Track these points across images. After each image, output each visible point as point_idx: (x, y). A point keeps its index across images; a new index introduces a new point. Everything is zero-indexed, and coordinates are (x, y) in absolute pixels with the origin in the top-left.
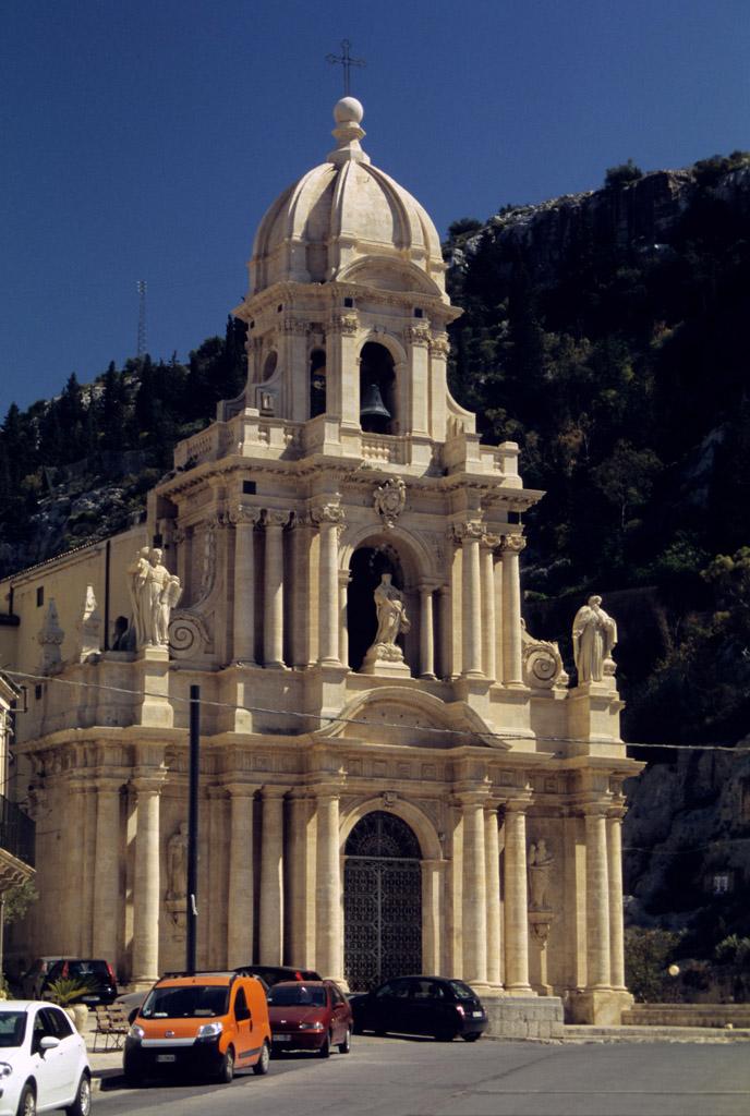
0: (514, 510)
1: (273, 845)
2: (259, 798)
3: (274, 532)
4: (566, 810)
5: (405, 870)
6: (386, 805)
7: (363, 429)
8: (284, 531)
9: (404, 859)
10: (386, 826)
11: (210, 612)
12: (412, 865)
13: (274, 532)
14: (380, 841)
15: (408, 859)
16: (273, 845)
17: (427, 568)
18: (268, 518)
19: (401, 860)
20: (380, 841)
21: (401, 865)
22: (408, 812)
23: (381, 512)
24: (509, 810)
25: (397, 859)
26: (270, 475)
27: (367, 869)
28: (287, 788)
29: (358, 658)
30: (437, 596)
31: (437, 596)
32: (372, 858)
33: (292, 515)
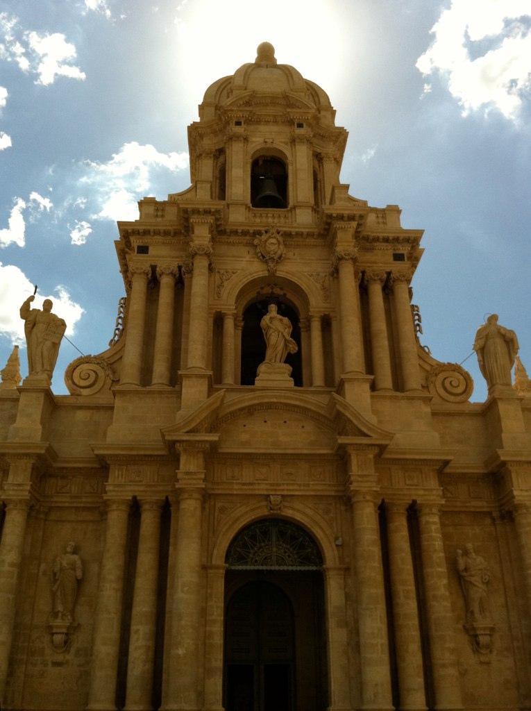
0: (397, 252)
1: (146, 560)
2: (135, 509)
3: (166, 283)
4: (495, 514)
6: (271, 509)
7: (253, 206)
8: (176, 284)
11: (118, 357)
13: (166, 283)
14: (275, 549)
16: (146, 560)
17: (316, 304)
20: (275, 549)
22: (299, 513)
23: (264, 257)
26: (159, 238)
29: (248, 376)
30: (326, 323)
31: (326, 323)
33: (180, 268)
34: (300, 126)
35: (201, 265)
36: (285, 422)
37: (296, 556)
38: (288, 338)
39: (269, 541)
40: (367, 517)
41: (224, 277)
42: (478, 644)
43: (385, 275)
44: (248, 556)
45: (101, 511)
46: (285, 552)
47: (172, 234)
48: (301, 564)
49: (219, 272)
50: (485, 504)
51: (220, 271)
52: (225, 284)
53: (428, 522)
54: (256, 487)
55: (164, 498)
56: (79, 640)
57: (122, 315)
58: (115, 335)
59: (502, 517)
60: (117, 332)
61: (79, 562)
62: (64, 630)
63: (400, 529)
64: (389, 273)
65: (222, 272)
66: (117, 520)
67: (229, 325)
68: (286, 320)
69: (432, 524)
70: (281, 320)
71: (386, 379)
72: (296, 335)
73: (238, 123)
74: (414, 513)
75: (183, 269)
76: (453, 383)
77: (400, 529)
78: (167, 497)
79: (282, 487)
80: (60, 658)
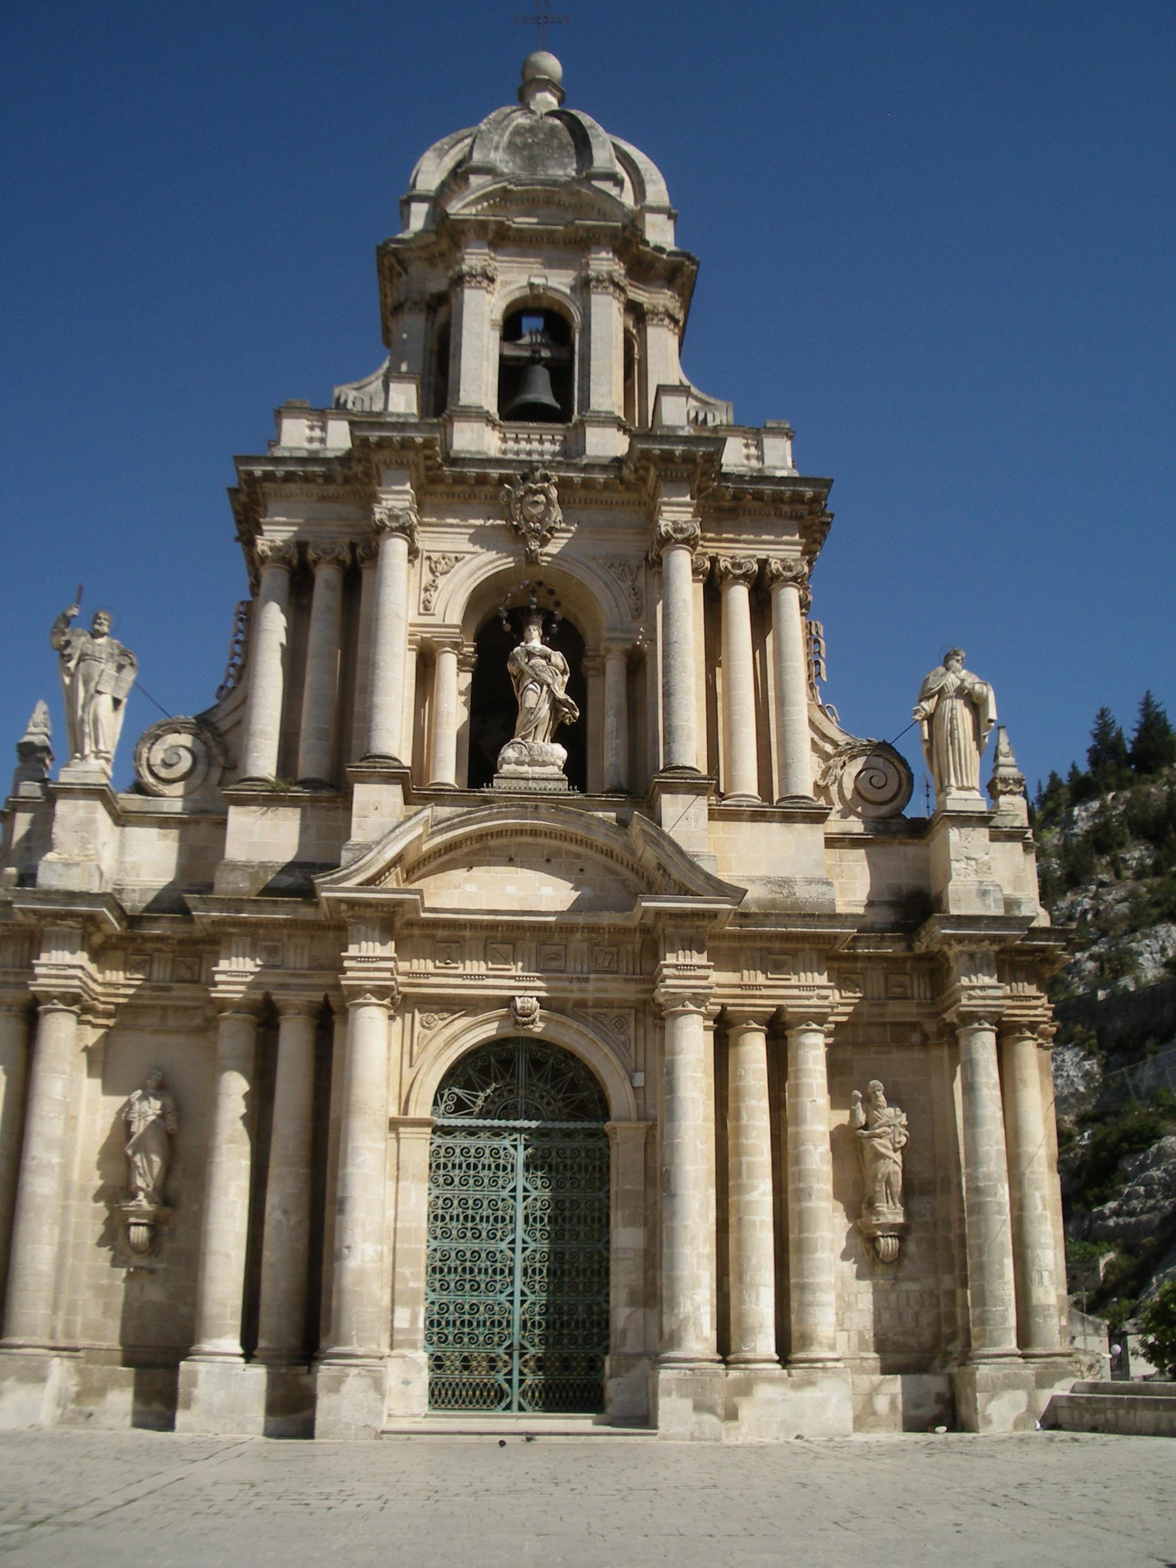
3: (325, 577)
4: (931, 1027)
5: (575, 1145)
9: (572, 1125)
10: (536, 1064)
12: (591, 1134)
15: (579, 1125)
18: (311, 555)
19: (564, 1125)
21: (568, 1134)
24: (790, 1026)
25: (557, 1125)
27: (496, 1143)
28: (319, 997)
32: (503, 1123)
33: (353, 547)
35: (396, 548)
36: (548, 860)
37: (560, 1104)
38: (561, 694)
39: (512, 1075)
41: (440, 568)
42: (877, 1252)
43: (756, 567)
44: (474, 1103)
46: (542, 1097)
48: (572, 1117)
49: (429, 558)
50: (914, 1010)
51: (432, 555)
52: (441, 581)
55: (321, 999)
57: (241, 637)
58: (229, 676)
59: (940, 1033)
60: (232, 670)
64: (763, 563)
65: (434, 556)
67: (448, 663)
68: (558, 658)
70: (547, 658)
72: (577, 687)
75: (359, 551)
76: (873, 780)
78: (326, 997)
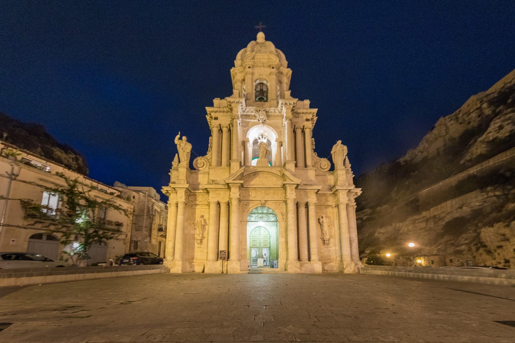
3: (225, 130)
4: (334, 206)
13: (225, 130)
34: (273, 68)
40: (291, 206)
42: (325, 243)
45: (208, 205)
47: (226, 112)
53: (311, 208)
54: (256, 198)
56: (205, 241)
61: (203, 220)
62: (200, 239)
63: (303, 210)
66: (213, 208)
69: (312, 209)
71: (301, 163)
73: (249, 67)
74: (307, 205)
77: (303, 210)
79: (265, 198)
80: (199, 246)
